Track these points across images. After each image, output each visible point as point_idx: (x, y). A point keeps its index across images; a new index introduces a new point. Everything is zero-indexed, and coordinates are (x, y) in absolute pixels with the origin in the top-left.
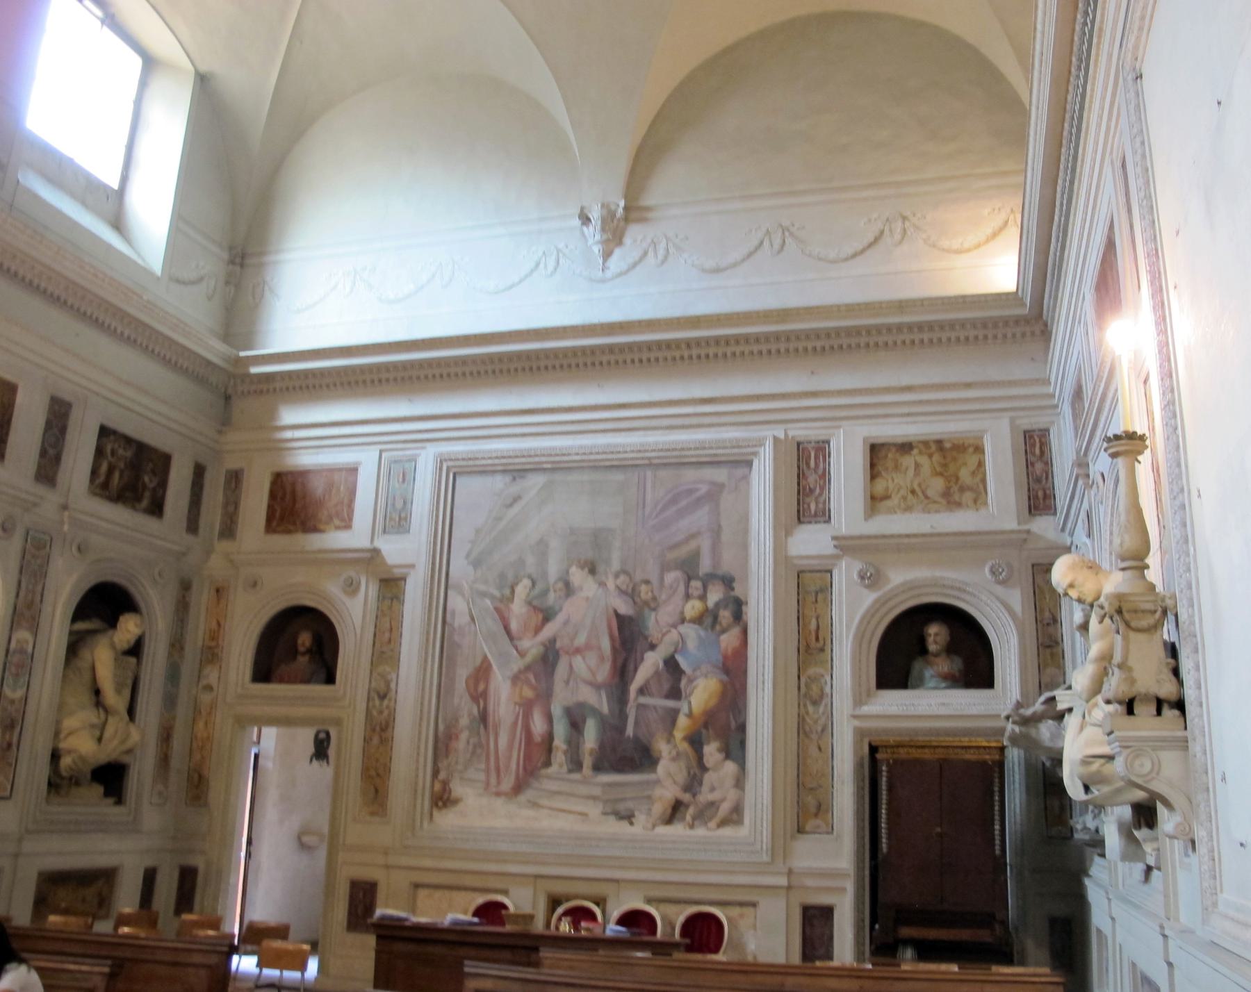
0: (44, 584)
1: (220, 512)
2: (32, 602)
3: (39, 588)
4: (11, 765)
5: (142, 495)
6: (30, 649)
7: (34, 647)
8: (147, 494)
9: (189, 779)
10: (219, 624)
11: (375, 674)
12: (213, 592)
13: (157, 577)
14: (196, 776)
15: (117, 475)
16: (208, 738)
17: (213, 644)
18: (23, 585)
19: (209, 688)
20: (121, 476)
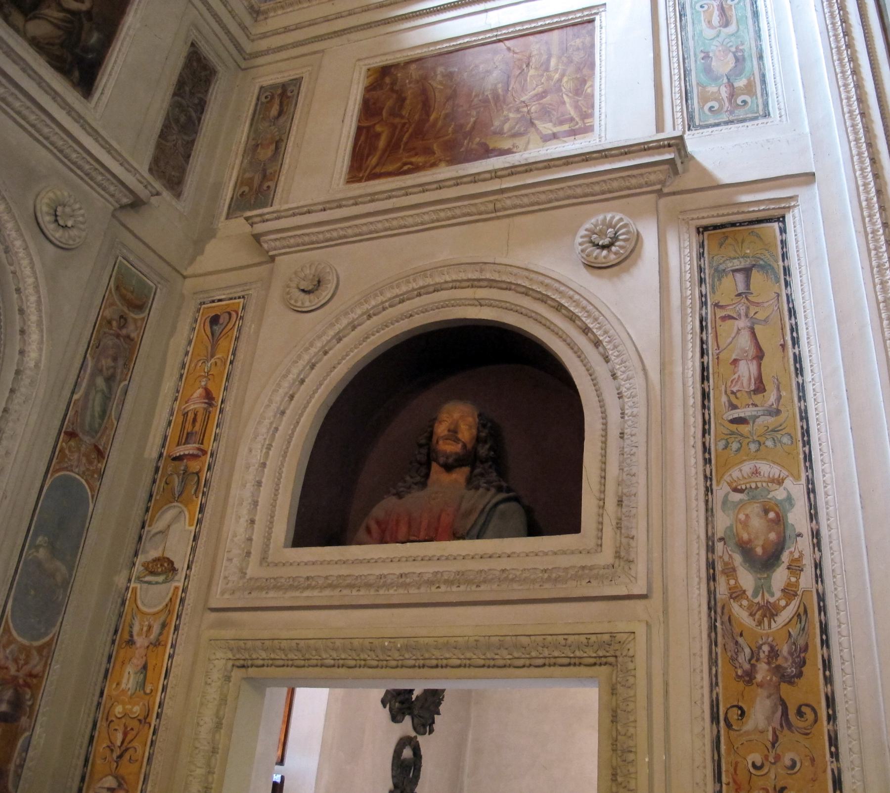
10: (209, 396)
11: (721, 491)
13: (46, 220)
16: (144, 720)
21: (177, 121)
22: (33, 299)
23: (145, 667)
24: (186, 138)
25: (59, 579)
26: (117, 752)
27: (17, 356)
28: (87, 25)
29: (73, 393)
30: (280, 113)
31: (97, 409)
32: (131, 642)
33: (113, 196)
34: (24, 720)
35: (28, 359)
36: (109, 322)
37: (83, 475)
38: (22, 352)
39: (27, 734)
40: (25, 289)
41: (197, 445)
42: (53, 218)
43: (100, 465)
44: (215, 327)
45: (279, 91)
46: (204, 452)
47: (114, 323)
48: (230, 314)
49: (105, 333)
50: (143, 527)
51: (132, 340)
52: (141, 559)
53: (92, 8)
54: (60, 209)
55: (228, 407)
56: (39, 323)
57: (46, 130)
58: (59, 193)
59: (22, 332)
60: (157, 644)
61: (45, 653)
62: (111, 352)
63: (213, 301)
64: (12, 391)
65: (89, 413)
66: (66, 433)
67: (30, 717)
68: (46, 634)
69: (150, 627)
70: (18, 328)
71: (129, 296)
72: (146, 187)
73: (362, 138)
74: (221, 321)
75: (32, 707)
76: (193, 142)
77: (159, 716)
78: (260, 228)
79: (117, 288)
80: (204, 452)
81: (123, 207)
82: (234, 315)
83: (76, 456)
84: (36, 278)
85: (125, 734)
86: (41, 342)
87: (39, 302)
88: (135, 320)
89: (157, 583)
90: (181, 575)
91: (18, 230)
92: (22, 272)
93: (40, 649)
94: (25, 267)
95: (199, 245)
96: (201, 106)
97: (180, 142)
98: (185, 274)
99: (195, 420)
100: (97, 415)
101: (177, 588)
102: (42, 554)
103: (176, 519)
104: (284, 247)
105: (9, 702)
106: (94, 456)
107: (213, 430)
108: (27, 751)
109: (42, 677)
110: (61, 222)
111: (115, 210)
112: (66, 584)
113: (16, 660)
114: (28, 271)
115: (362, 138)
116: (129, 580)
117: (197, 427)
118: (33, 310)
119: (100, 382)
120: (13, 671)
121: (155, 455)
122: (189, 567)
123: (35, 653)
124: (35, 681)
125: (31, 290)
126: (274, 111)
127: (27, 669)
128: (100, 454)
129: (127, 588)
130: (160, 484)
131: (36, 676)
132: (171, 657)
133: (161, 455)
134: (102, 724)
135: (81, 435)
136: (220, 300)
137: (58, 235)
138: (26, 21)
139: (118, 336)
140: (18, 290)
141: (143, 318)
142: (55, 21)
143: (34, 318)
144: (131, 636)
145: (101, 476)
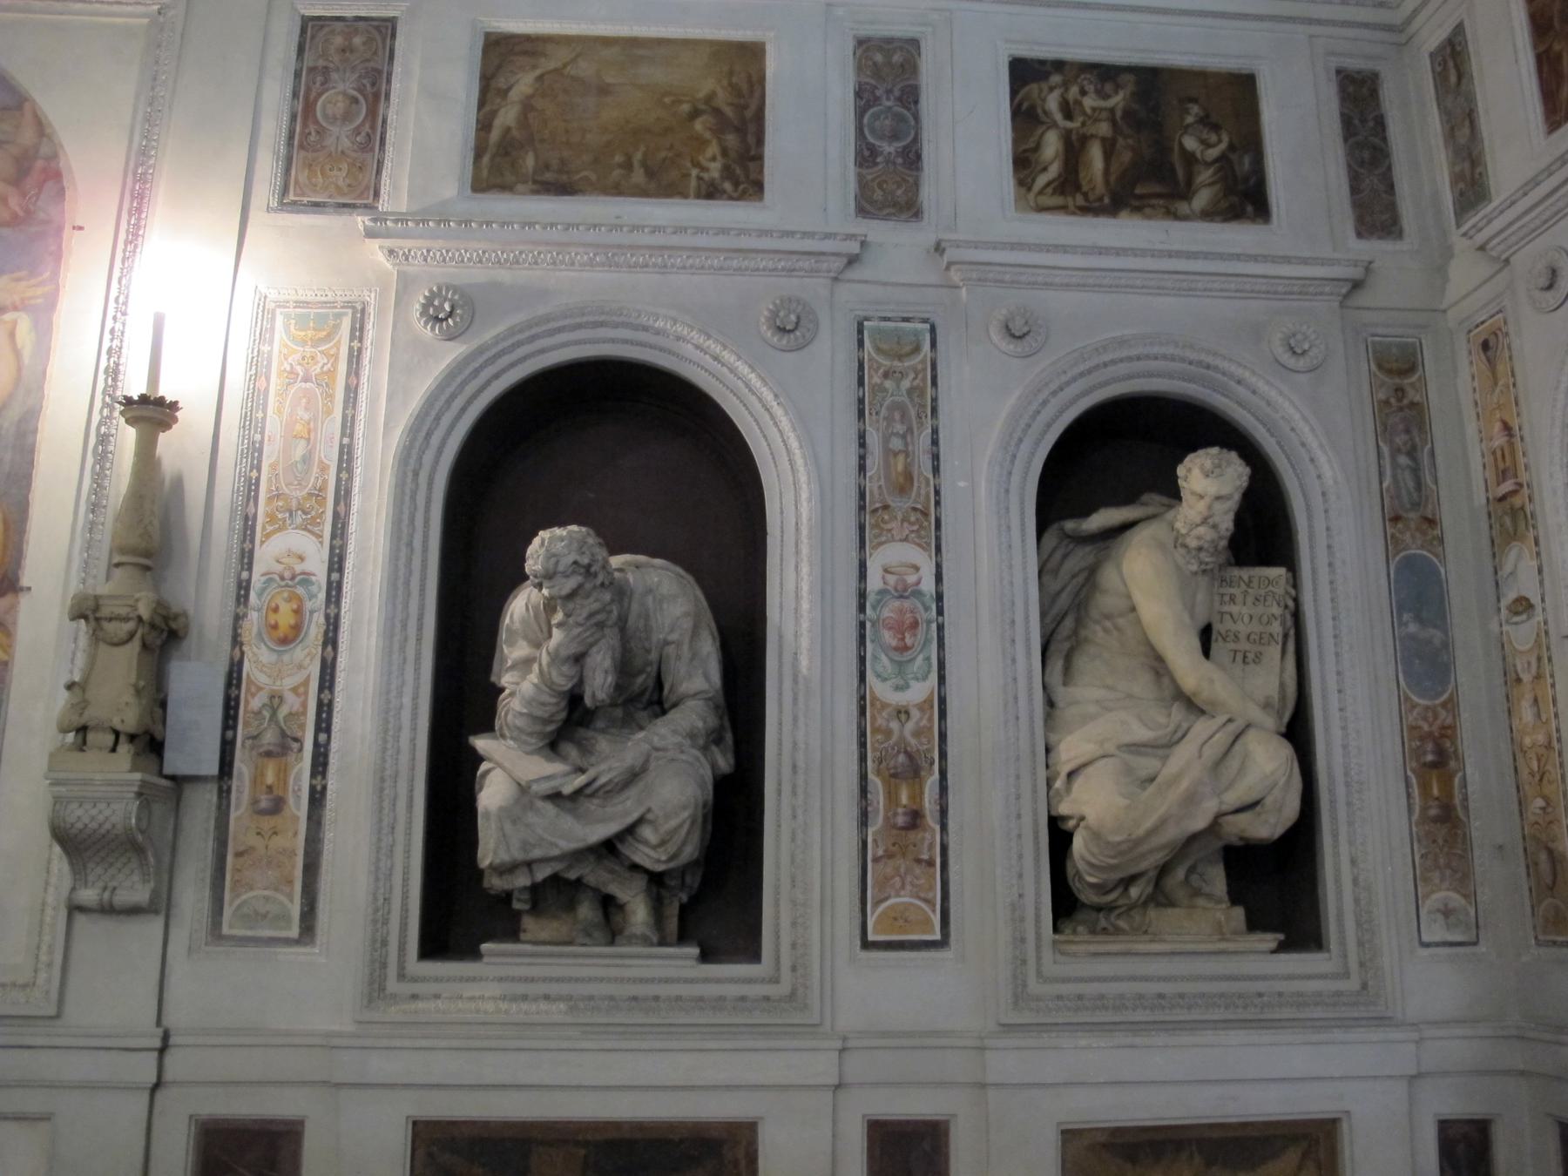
0: (935, 431)
1: (1443, 156)
2: (908, 476)
3: (924, 439)
4: (931, 863)
5: (1189, 181)
6: (928, 586)
7: (939, 578)
8: (1205, 175)
9: (1532, 866)
10: (1507, 428)
12: (1480, 358)
13: (1286, 358)
14: (1543, 857)
15: (1096, 154)
16: (1549, 746)
17: (1508, 486)
18: (873, 439)
19: (1523, 606)
20: (1109, 154)
21: (1362, 163)
22: (1307, 429)
23: (1536, 700)
24: (1377, 172)
25: (1437, 642)
26: (1537, 777)
28: (1234, 157)
29: (1381, 483)
30: (1460, 77)
31: (1411, 484)
32: (1519, 680)
33: (1332, 294)
34: (1453, 764)
36: (1387, 402)
37: (1422, 547)
38: (1319, 477)
39: (1460, 774)
41: (1512, 481)
42: (1289, 354)
43: (1435, 532)
44: (1489, 353)
45: (1448, 50)
46: (1521, 485)
47: (1393, 400)
48: (1496, 335)
49: (1387, 414)
50: (1496, 573)
51: (1418, 404)
52: (1504, 603)
53: (1231, 139)
54: (1292, 342)
55: (1526, 432)
56: (1321, 446)
57: (1248, 287)
58: (1285, 330)
59: (1312, 460)
60: (1538, 677)
61: (1449, 706)
62: (1401, 427)
63: (1477, 326)
64: (1326, 511)
65: (1404, 492)
66: (1391, 520)
67: (1457, 759)
68: (1444, 691)
69: (1529, 663)
70: (1307, 460)
71: (1395, 366)
72: (1356, 266)
73: (1545, 69)
74: (1491, 344)
75: (1456, 751)
76: (1389, 168)
77: (1559, 740)
78: (1480, 238)
79: (1380, 367)
80: (1521, 485)
81: (1346, 296)
82: (1499, 332)
83: (1408, 535)
84: (1301, 412)
85: (1539, 760)
86: (1329, 461)
87: (1313, 430)
88: (1412, 385)
89: (1523, 622)
90: (1539, 609)
91: (1268, 382)
93: (1444, 705)
95: (1439, 272)
96: (1380, 123)
97: (1376, 181)
98: (1443, 307)
99: (1503, 456)
100: (1412, 490)
101: (1539, 623)
102: (1413, 628)
103: (1519, 557)
104: (1510, 247)
105: (1433, 752)
106: (1425, 526)
107: (1521, 461)
108: (1465, 787)
109: (1455, 727)
110: (1299, 351)
111: (1341, 303)
112: (1446, 645)
113: (1425, 719)
114: (1291, 411)
115: (1545, 69)
116: (1501, 625)
117: (1508, 464)
119: (1403, 460)
120: (1426, 727)
121: (1484, 501)
122: (1543, 600)
123: (1439, 709)
124: (1449, 732)
126: (1453, 79)
127: (1438, 722)
128: (1431, 522)
129: (1502, 633)
130: (1497, 527)
131: (1449, 727)
132: (1553, 686)
133: (1488, 499)
134: (1519, 756)
135: (1405, 515)
136: (1483, 323)
137: (1301, 363)
138: (1190, 204)
139: (1401, 409)
140: (1293, 429)
141: (1420, 377)
142: (1211, 180)
144: (1517, 674)
145: (1441, 541)
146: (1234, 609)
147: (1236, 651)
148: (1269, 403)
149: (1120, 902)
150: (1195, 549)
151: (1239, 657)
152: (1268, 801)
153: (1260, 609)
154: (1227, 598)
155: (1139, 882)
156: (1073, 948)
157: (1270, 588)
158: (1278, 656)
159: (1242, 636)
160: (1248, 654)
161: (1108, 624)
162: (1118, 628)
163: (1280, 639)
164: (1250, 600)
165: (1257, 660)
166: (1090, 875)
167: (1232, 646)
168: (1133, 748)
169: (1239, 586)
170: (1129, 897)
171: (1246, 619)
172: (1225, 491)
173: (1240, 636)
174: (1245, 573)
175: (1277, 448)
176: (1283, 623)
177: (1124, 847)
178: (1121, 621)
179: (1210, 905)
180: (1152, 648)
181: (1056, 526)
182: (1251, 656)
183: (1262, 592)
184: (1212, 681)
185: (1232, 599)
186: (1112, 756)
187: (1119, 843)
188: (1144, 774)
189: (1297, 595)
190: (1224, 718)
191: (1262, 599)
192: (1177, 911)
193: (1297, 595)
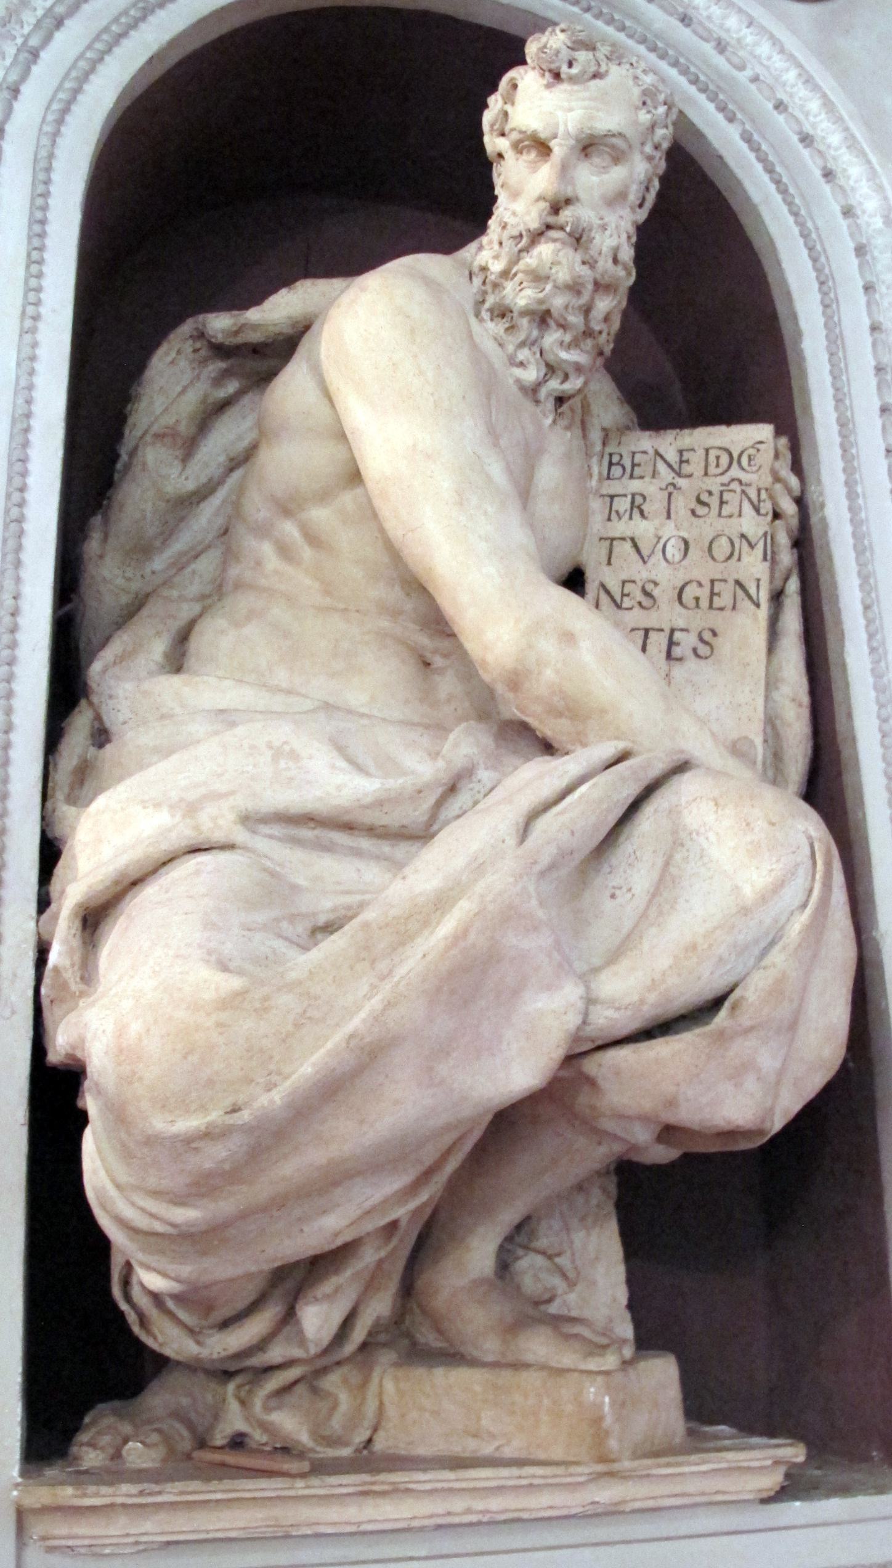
22: (814, 105)
27: (843, 223)
35: (866, 218)
38: (848, 212)
40: (791, 96)
56: (851, 142)
59: (828, 174)
64: (868, 288)
84: (800, 66)
87: (828, 105)
92: (767, 68)
94: (769, 58)
114: (778, 62)
118: (825, 125)
125: (802, 92)
140: (780, 106)
143: (835, 139)
146: (642, 528)
147: (647, 631)
148: (721, 47)
149: (276, 1354)
150: (526, 312)
151: (658, 642)
152: (752, 992)
153: (709, 526)
154: (623, 505)
155: (327, 1287)
156: (85, 1530)
157: (735, 472)
158: (759, 639)
159: (664, 594)
160: (678, 635)
161: (289, 529)
162: (313, 539)
163: (764, 597)
164: (681, 504)
165: (703, 650)
166: (148, 1268)
167: (636, 618)
168: (306, 833)
169: (655, 474)
170: (301, 1340)
171: (674, 551)
172: (608, 121)
173: (656, 592)
174: (670, 443)
175: (744, 146)
176: (769, 556)
177: (216, 1155)
178: (320, 515)
179: (568, 1359)
180: (394, 554)
181: (187, 327)
182: (687, 641)
183: (714, 484)
184: (568, 638)
185: (637, 507)
186: (228, 847)
187: (190, 1142)
188: (325, 906)
189: (803, 491)
190: (607, 749)
191: (714, 502)
192: (461, 1376)
193: (803, 491)
